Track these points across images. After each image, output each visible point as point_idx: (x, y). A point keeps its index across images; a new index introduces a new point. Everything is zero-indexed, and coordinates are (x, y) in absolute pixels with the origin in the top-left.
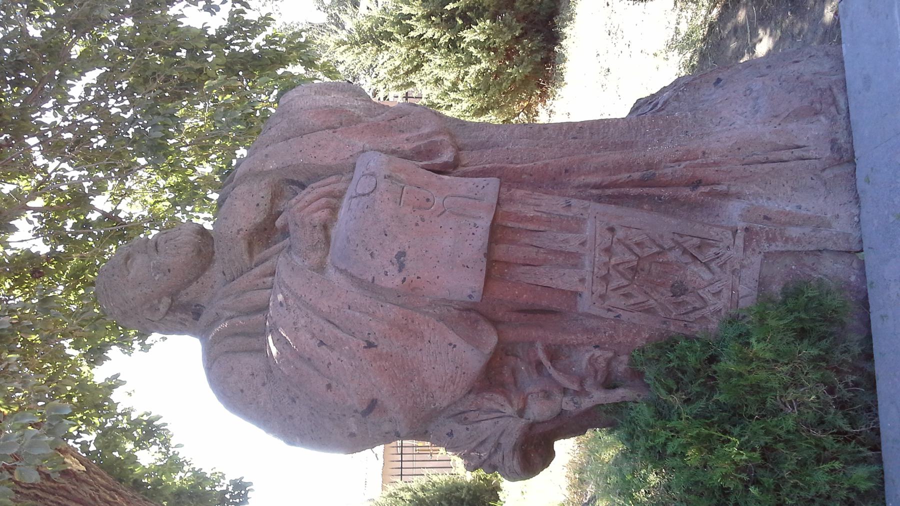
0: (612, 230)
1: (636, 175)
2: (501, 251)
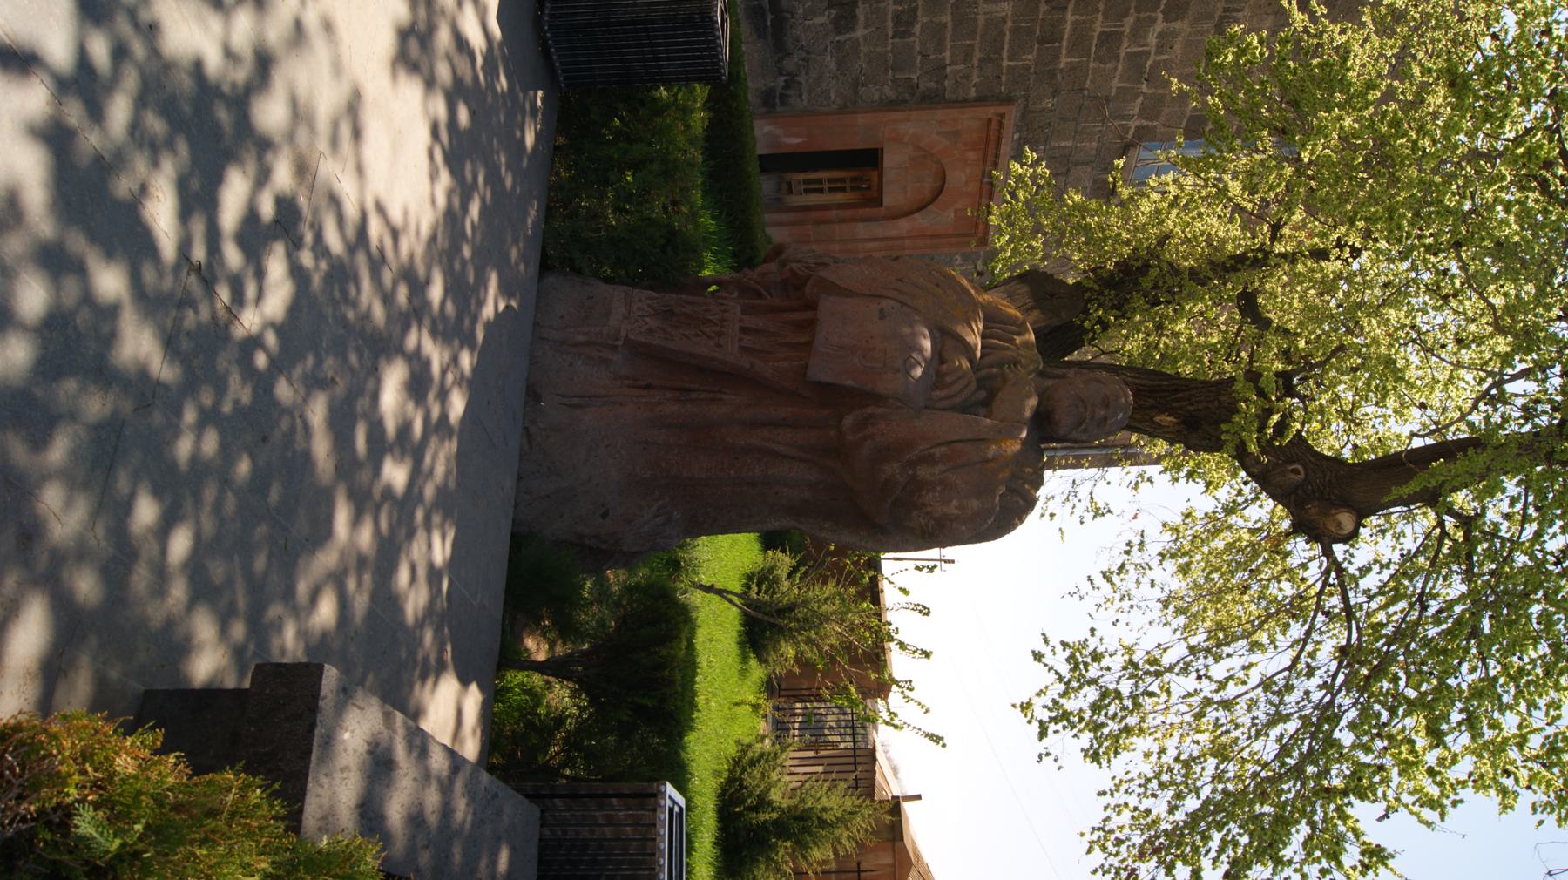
0: (719, 346)
1: (694, 395)
2: (804, 339)
